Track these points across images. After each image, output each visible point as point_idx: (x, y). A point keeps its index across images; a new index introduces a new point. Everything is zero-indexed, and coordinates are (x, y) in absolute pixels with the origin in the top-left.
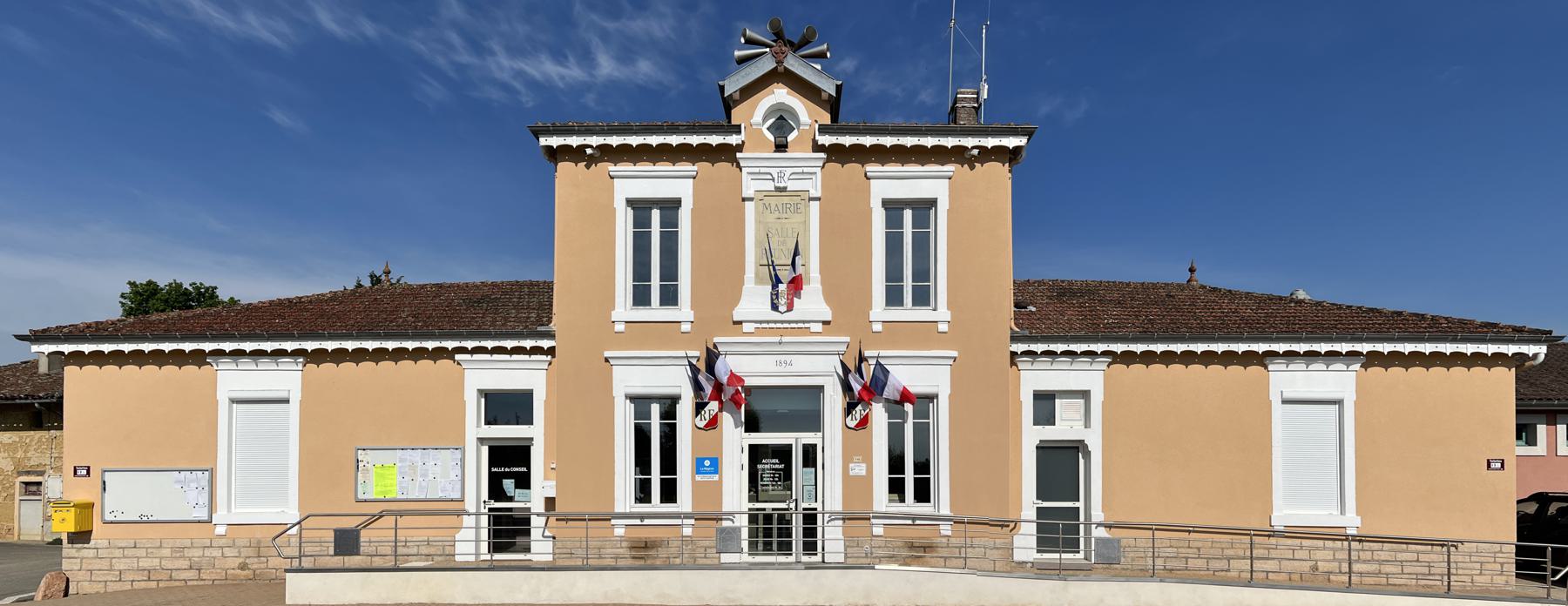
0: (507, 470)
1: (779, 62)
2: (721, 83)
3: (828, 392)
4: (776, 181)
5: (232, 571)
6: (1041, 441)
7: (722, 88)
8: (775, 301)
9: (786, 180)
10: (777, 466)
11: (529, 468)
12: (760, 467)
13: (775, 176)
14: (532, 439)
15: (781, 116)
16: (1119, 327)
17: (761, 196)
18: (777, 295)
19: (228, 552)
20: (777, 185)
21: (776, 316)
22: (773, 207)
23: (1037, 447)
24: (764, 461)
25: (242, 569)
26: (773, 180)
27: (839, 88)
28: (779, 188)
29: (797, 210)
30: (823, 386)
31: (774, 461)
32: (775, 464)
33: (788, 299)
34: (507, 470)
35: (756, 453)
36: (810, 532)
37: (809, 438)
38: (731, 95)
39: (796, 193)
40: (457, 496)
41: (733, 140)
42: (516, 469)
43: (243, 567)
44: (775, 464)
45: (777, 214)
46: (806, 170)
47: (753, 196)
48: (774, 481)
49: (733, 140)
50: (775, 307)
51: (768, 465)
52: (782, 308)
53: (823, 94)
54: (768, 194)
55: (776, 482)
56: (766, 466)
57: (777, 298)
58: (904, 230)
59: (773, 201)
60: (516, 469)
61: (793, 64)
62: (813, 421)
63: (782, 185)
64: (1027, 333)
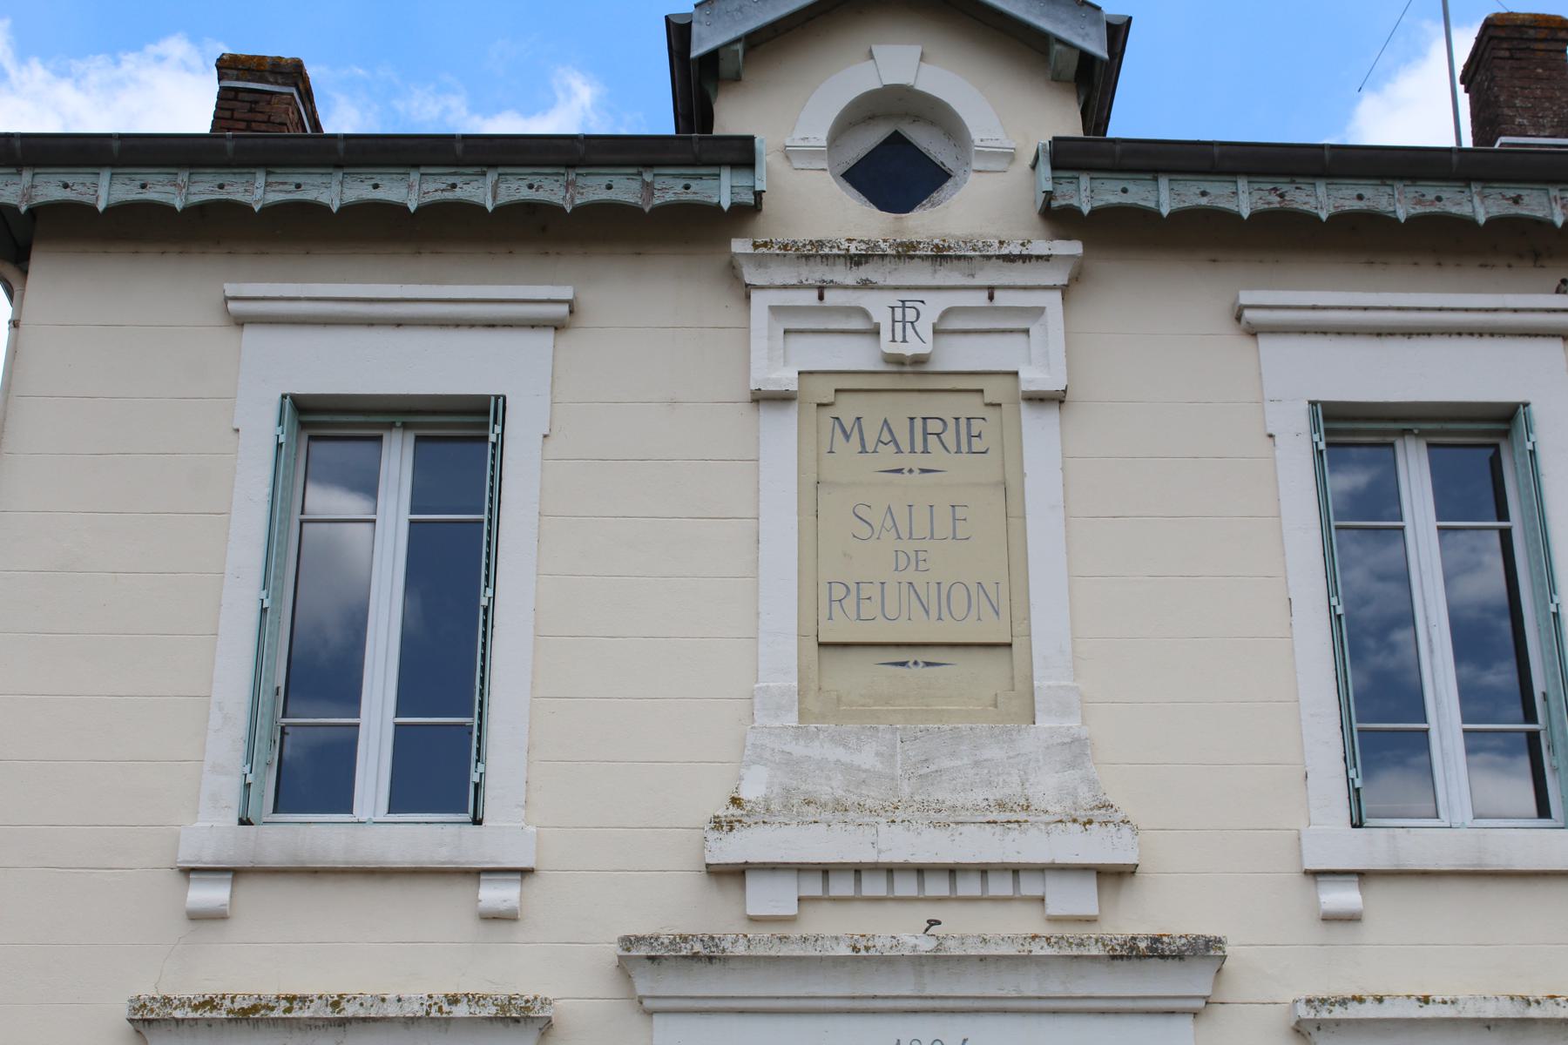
4: (885, 334)
9: (927, 333)
13: (882, 317)
17: (823, 390)
20: (887, 346)
22: (871, 432)
26: (875, 332)
28: (898, 360)
29: (967, 438)
38: (713, 57)
39: (970, 383)
41: (724, 190)
45: (888, 457)
46: (1002, 299)
47: (794, 387)
49: (724, 190)
54: (850, 385)
58: (1407, 523)
59: (873, 411)
63: (911, 348)
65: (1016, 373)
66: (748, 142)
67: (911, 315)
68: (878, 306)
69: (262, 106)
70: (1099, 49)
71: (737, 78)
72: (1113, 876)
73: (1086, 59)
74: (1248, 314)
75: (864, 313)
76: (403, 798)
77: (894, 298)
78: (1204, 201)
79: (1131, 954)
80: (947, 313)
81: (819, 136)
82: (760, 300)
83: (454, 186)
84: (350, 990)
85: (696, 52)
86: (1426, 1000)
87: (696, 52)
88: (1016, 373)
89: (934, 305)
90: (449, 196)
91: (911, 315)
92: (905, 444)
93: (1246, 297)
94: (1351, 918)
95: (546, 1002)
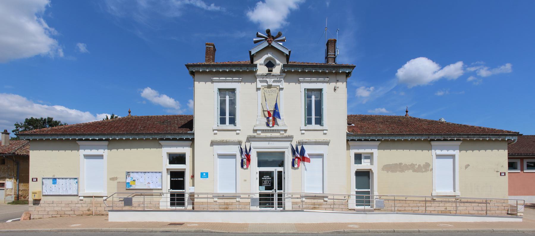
0: (176, 179)
1: (270, 44)
2: (250, 51)
3: (286, 154)
4: (268, 82)
5: (85, 212)
6: (357, 169)
7: (250, 52)
8: (268, 123)
10: (269, 178)
11: (184, 179)
12: (263, 178)
13: (268, 81)
14: (185, 169)
15: (270, 61)
16: (383, 131)
18: (269, 121)
19: (84, 205)
21: (269, 128)
23: (356, 172)
24: (264, 177)
25: (88, 211)
27: (290, 52)
30: (285, 152)
31: (268, 177)
32: (268, 178)
33: (273, 122)
34: (176, 179)
35: (262, 174)
36: (280, 200)
37: (280, 169)
38: (253, 55)
40: (160, 188)
42: (180, 179)
43: (89, 210)
44: (268, 178)
48: (268, 183)
50: (268, 125)
51: (266, 178)
52: (271, 125)
53: (284, 54)
55: (269, 183)
56: (265, 178)
57: (269, 122)
60: (180, 179)
61: (274, 44)
62: (281, 164)
64: (352, 133)
65: (279, 86)
66: (256, 65)
67: (271, 80)
68: (268, 80)
69: (210, 49)
70: (288, 54)
71: (255, 56)
72: (285, 131)
73: (287, 55)
74: (300, 80)
75: (267, 81)
76: (230, 123)
77: (269, 79)
78: (296, 70)
79: (286, 137)
80: (274, 81)
81: (263, 62)
82: (258, 79)
83: (231, 69)
84: (227, 139)
85: (252, 54)
86: (309, 140)
87: (252, 54)
88: (279, 86)
89: (273, 80)
90: (230, 70)
91: (271, 80)
92: (270, 92)
93: (300, 79)
94: (304, 134)
95: (242, 140)
